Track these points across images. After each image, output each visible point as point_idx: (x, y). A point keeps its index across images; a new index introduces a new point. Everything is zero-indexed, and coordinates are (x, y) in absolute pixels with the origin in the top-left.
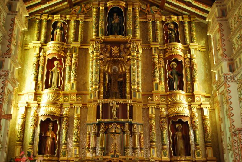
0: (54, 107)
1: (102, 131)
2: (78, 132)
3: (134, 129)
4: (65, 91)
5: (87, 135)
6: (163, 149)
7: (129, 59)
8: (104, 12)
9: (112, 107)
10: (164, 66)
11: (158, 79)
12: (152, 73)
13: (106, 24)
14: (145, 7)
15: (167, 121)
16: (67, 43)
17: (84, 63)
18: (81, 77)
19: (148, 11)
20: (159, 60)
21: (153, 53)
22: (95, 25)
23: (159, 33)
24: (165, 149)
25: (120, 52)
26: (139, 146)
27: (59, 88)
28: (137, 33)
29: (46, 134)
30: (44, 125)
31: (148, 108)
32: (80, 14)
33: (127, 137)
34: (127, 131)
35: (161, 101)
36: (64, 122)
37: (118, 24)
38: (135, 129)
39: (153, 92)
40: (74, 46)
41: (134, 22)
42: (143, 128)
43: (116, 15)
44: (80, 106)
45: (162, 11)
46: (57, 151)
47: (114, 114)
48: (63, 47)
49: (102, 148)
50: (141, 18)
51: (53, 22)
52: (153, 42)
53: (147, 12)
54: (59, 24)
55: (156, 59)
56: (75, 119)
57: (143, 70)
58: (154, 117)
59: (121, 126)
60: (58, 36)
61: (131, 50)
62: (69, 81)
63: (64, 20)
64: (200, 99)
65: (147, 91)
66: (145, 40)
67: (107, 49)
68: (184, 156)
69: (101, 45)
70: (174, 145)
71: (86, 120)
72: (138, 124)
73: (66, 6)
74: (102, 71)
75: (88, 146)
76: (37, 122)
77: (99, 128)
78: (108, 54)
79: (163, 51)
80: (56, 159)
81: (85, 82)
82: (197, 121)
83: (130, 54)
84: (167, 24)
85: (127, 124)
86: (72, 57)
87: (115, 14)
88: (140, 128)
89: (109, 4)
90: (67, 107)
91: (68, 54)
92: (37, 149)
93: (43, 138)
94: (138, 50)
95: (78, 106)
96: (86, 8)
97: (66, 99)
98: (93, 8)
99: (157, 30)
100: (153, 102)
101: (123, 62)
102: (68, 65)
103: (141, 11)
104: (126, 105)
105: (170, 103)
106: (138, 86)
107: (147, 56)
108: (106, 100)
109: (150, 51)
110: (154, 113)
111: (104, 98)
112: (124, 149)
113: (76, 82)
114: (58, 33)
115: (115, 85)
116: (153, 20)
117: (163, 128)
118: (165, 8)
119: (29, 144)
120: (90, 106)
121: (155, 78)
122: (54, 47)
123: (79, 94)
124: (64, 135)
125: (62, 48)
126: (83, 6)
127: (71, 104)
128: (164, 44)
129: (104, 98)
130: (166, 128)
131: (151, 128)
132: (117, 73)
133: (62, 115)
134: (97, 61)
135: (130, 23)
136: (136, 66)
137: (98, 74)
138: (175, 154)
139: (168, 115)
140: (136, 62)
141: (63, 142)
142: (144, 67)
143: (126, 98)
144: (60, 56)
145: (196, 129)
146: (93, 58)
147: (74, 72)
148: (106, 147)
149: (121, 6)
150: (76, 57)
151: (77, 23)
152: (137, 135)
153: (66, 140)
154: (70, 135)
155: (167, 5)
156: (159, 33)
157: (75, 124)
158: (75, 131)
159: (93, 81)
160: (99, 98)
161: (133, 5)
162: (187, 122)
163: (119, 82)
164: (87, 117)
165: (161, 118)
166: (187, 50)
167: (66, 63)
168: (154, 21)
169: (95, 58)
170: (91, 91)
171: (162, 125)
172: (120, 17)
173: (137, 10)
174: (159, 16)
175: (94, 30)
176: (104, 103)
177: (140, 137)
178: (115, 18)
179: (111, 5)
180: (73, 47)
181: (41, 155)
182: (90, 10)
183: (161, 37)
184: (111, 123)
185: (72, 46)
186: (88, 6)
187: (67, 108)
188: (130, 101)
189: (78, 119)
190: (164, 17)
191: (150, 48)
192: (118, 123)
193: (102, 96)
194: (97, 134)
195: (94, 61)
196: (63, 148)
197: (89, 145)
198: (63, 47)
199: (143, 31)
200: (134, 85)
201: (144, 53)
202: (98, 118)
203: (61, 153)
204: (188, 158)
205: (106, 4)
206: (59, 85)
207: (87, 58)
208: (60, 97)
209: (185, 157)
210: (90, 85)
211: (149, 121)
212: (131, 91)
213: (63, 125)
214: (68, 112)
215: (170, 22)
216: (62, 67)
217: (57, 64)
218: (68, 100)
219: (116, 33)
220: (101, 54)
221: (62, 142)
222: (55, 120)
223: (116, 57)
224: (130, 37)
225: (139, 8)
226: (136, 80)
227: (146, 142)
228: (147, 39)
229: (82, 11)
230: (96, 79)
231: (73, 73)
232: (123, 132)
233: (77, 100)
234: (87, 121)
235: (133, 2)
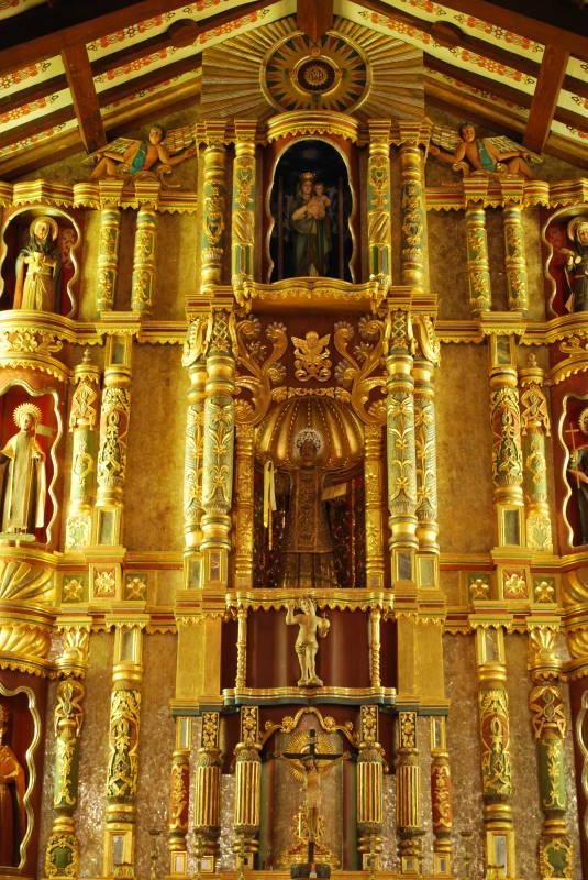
0: (15, 629)
1: (249, 748)
3: (405, 738)
4: (66, 551)
5: (175, 767)
6: (547, 836)
7: (377, 395)
8: (253, 167)
9: (293, 629)
10: (548, 426)
11: (517, 490)
12: (488, 462)
13: (263, 224)
14: (455, 139)
15: (567, 699)
16: (76, 317)
17: (161, 413)
18: (143, 481)
19: (466, 159)
20: (525, 396)
21: (496, 363)
22: (214, 230)
23: (525, 269)
24: (559, 836)
25: (335, 358)
26: (428, 823)
27: (40, 534)
28: (414, 267)
31: (473, 633)
32: (142, 179)
33: (370, 773)
34: (369, 748)
35: (536, 597)
36: (62, 704)
37: (321, 222)
38: (408, 735)
39: (495, 552)
40: (110, 332)
41: (402, 213)
42: (448, 733)
43: (315, 182)
44: (142, 626)
45: (536, 159)
47: (308, 662)
48: (56, 338)
49: (245, 831)
50: (432, 192)
51: (11, 218)
52: (493, 309)
53: (464, 165)
54: (38, 228)
55: (508, 391)
56: (117, 686)
57: (444, 446)
58: (502, 677)
59: (339, 722)
61: (386, 350)
62: (84, 503)
63: (62, 207)
65: (468, 549)
67: (269, 344)
69: (244, 324)
71: (167, 693)
72: (424, 713)
73: (70, 141)
74: (247, 451)
75: (177, 822)
77: (233, 735)
78: (273, 372)
79: (545, 351)
81: (162, 507)
83: (380, 371)
84: (563, 223)
85: (369, 713)
86: (99, 386)
87: (308, 176)
89: (278, 128)
90: (78, 628)
91: (80, 371)
94: (420, 349)
95: (130, 625)
96: (165, 149)
97: (73, 589)
98: (203, 146)
99: (512, 250)
100: (495, 602)
101: (347, 406)
102: (81, 422)
103: (431, 158)
104: (363, 617)
105: (578, 608)
106: (422, 527)
107: (463, 377)
108: (266, 592)
109: (480, 355)
110: (502, 659)
111: (256, 585)
112: (355, 838)
113: (120, 505)
114: (34, 268)
115: (313, 520)
116: (495, 204)
117: (544, 731)
118: (552, 142)
120: (190, 622)
121: (506, 485)
122: (12, 337)
123: (134, 567)
124: (60, 768)
125: (54, 344)
126: (153, 140)
127: (97, 615)
128: (548, 317)
129: (256, 585)
130: (562, 731)
132: (320, 461)
133: (51, 668)
134: (221, 405)
136: (410, 429)
137: (228, 468)
139: (568, 669)
140: (410, 408)
141: (57, 802)
142: (449, 432)
143: (361, 583)
144: (43, 381)
146: (202, 387)
147: (109, 459)
148: (265, 830)
149: (337, 138)
150: (122, 386)
151: (126, 218)
153: (73, 789)
155: (558, 128)
156: (525, 269)
157: (116, 713)
158: (115, 745)
159: (205, 500)
160: (231, 585)
161: (396, 132)
163: (327, 504)
164: (173, 682)
165: (536, 684)
167: (72, 416)
168: (500, 208)
169: (210, 388)
170: (195, 549)
171: (540, 719)
172: (332, 191)
173: (416, 157)
174: (523, 183)
175: (207, 255)
176: (256, 608)
177: (434, 778)
178: (306, 197)
179: (290, 134)
180: (104, 337)
182: (189, 155)
183: (535, 287)
184: (291, 708)
185: (100, 332)
186: (179, 140)
187: (78, 634)
188: (380, 599)
189: (131, 687)
190: (544, 187)
191: (478, 340)
192: (328, 708)
193: (246, 572)
194: (223, 764)
195: (209, 404)
196: (56, 828)
197: (184, 817)
198: (56, 338)
199: (443, 255)
200: (403, 519)
201: (450, 362)
202: (227, 681)
205: (262, 130)
206: (40, 523)
207: (172, 388)
208: (44, 579)
210: (189, 521)
211: (476, 696)
212: (386, 552)
213: (57, 715)
214: (81, 654)
215: (573, 210)
216: (55, 434)
217: (27, 418)
218: (83, 596)
219: (313, 270)
220: (241, 370)
222: (18, 691)
223: (313, 383)
224: (380, 285)
225: (422, 147)
226: (412, 493)
227: (464, 801)
228: (465, 297)
229: (148, 164)
230: (218, 491)
231: (107, 462)
232: (352, 751)
233: (126, 594)
234: (173, 696)
235: (395, 119)
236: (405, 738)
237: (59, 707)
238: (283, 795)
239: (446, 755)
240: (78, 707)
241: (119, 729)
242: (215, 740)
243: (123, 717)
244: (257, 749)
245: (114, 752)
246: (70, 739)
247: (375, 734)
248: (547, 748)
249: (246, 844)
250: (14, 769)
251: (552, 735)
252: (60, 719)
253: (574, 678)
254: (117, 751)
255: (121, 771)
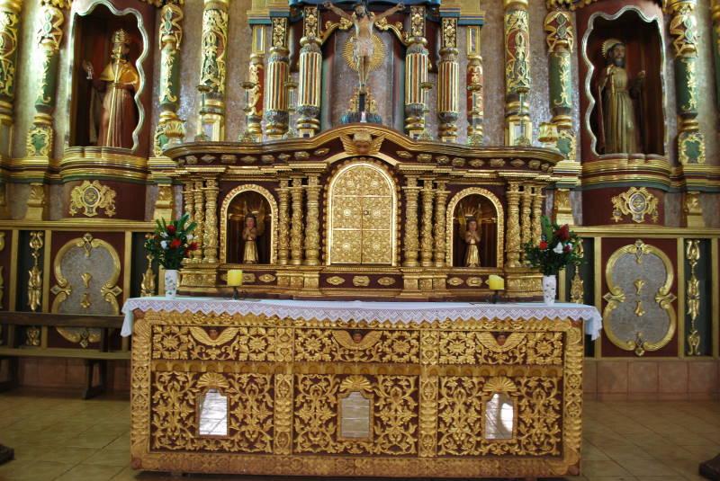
1: (311, 41)
2: (219, 59)
3: (447, 40)
15: (574, 23)
29: (104, 73)
34: (417, 42)
38: (450, 37)
46: (140, 136)
56: (207, 7)
68: (643, 155)
70: (600, 118)
75: (253, 111)
76: (63, 26)
80: (139, 162)
85: (417, 12)
88: (472, 43)
92: (65, 126)
119: (35, 111)
124: (165, 72)
130: (571, 47)
131: (515, 44)
138: (600, 150)
141: (162, 99)
145: (687, 55)
152: (456, 64)
153: (175, 88)
154: (190, 72)
157: (206, 28)
158: (207, 51)
162: (655, 22)
165: (550, 10)
171: (554, 36)
181: (78, 148)
194: (289, 66)
197: (259, 106)
203: (155, 143)
204: (656, 163)
209: (647, 160)
211: (503, 19)
213: (161, 32)
221: (158, 100)
222: (127, 11)
236: (447, 40)
237: (162, 26)
238: (341, 83)
239: (480, 58)
240: (177, 25)
241: (208, 40)
242: (283, 41)
243: (211, 31)
244: (318, 43)
245: (204, 58)
246: (171, 50)
247: (423, 30)
248: (559, 59)
249: (307, 121)
250: (134, 79)
251: (562, 50)
252: (163, 35)
253: (581, 6)
254: (207, 58)
255: (210, 73)
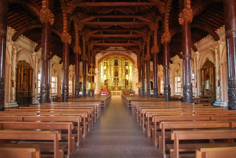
30: (105, 81)
60: (106, 65)
64: (131, 76)
66: (121, 66)
70: (126, 84)
82: (130, 80)
93: (105, 83)
112: (118, 85)
115: (116, 74)
135: (119, 63)
151: (109, 62)
166: (129, 67)
